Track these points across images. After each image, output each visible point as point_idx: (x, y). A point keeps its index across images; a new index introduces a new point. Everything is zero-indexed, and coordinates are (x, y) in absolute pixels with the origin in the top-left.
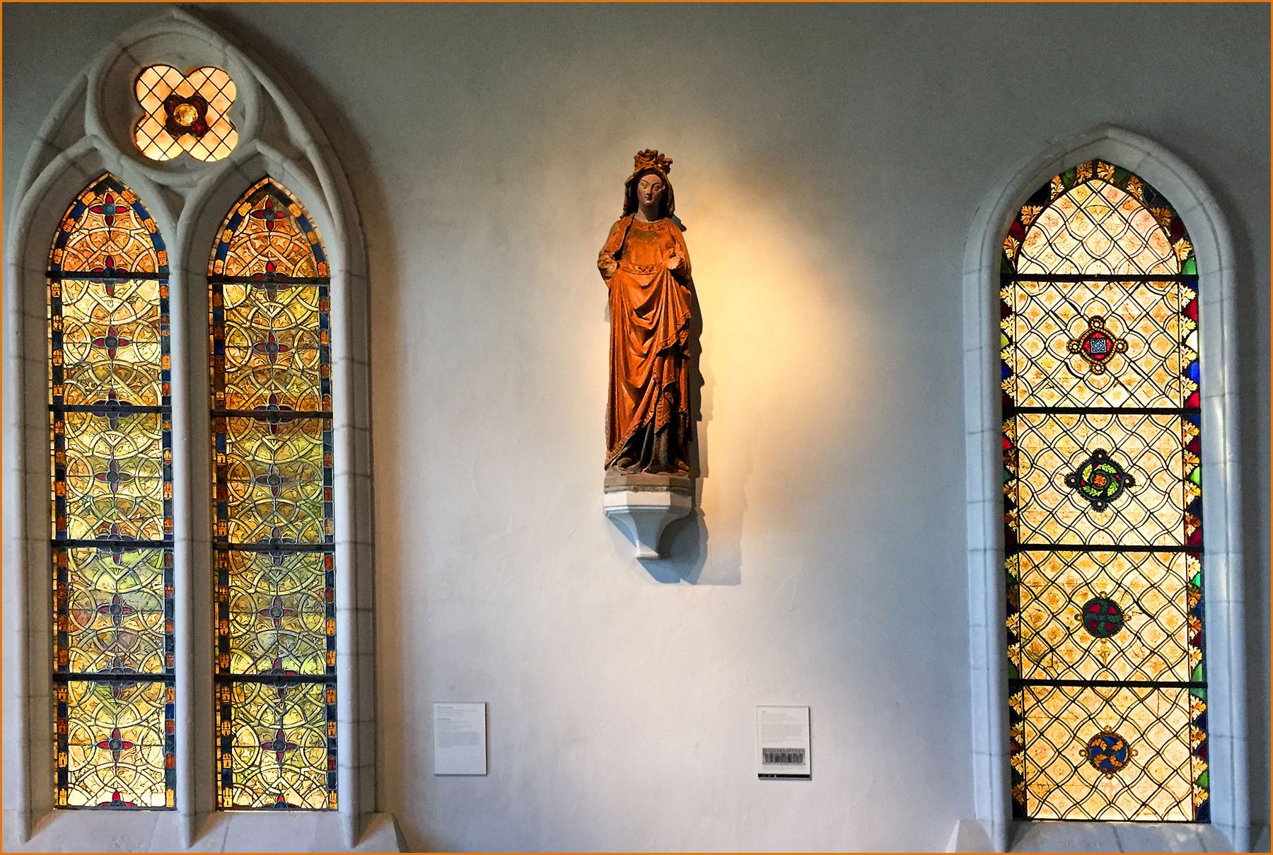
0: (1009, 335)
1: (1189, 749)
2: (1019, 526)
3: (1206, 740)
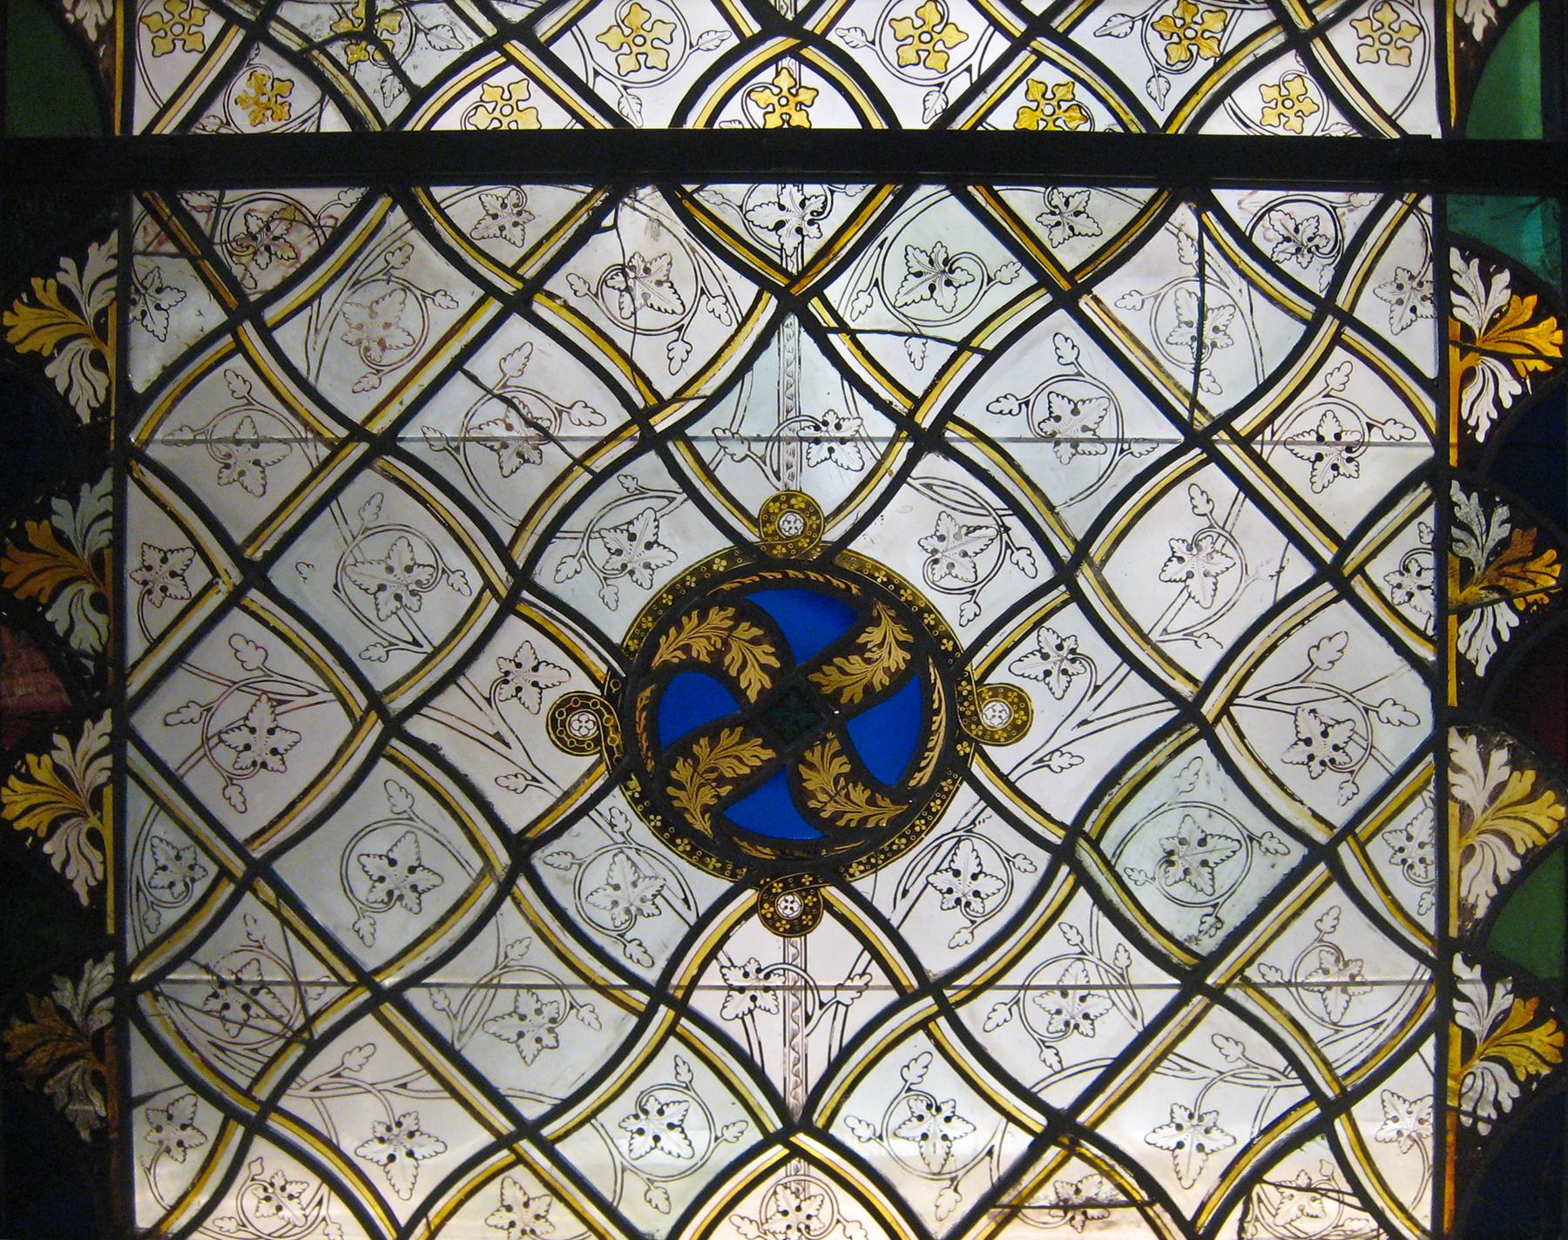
1: (1433, 676)
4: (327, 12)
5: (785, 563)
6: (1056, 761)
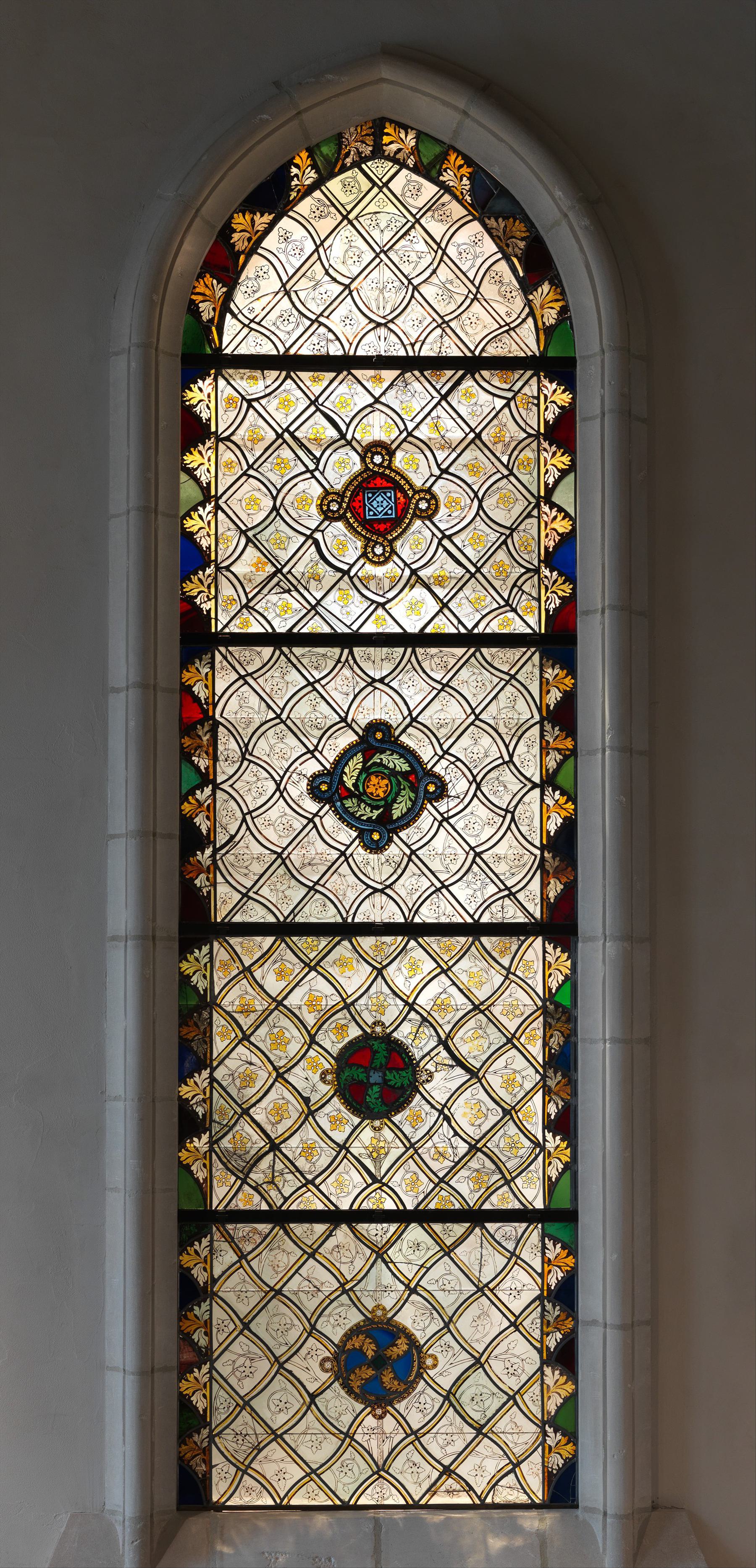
0: (204, 480)
1: (540, 1351)
2: (214, 884)
3: (574, 1331)
4: (262, 1176)
5: (378, 1323)
6: (445, 1374)
